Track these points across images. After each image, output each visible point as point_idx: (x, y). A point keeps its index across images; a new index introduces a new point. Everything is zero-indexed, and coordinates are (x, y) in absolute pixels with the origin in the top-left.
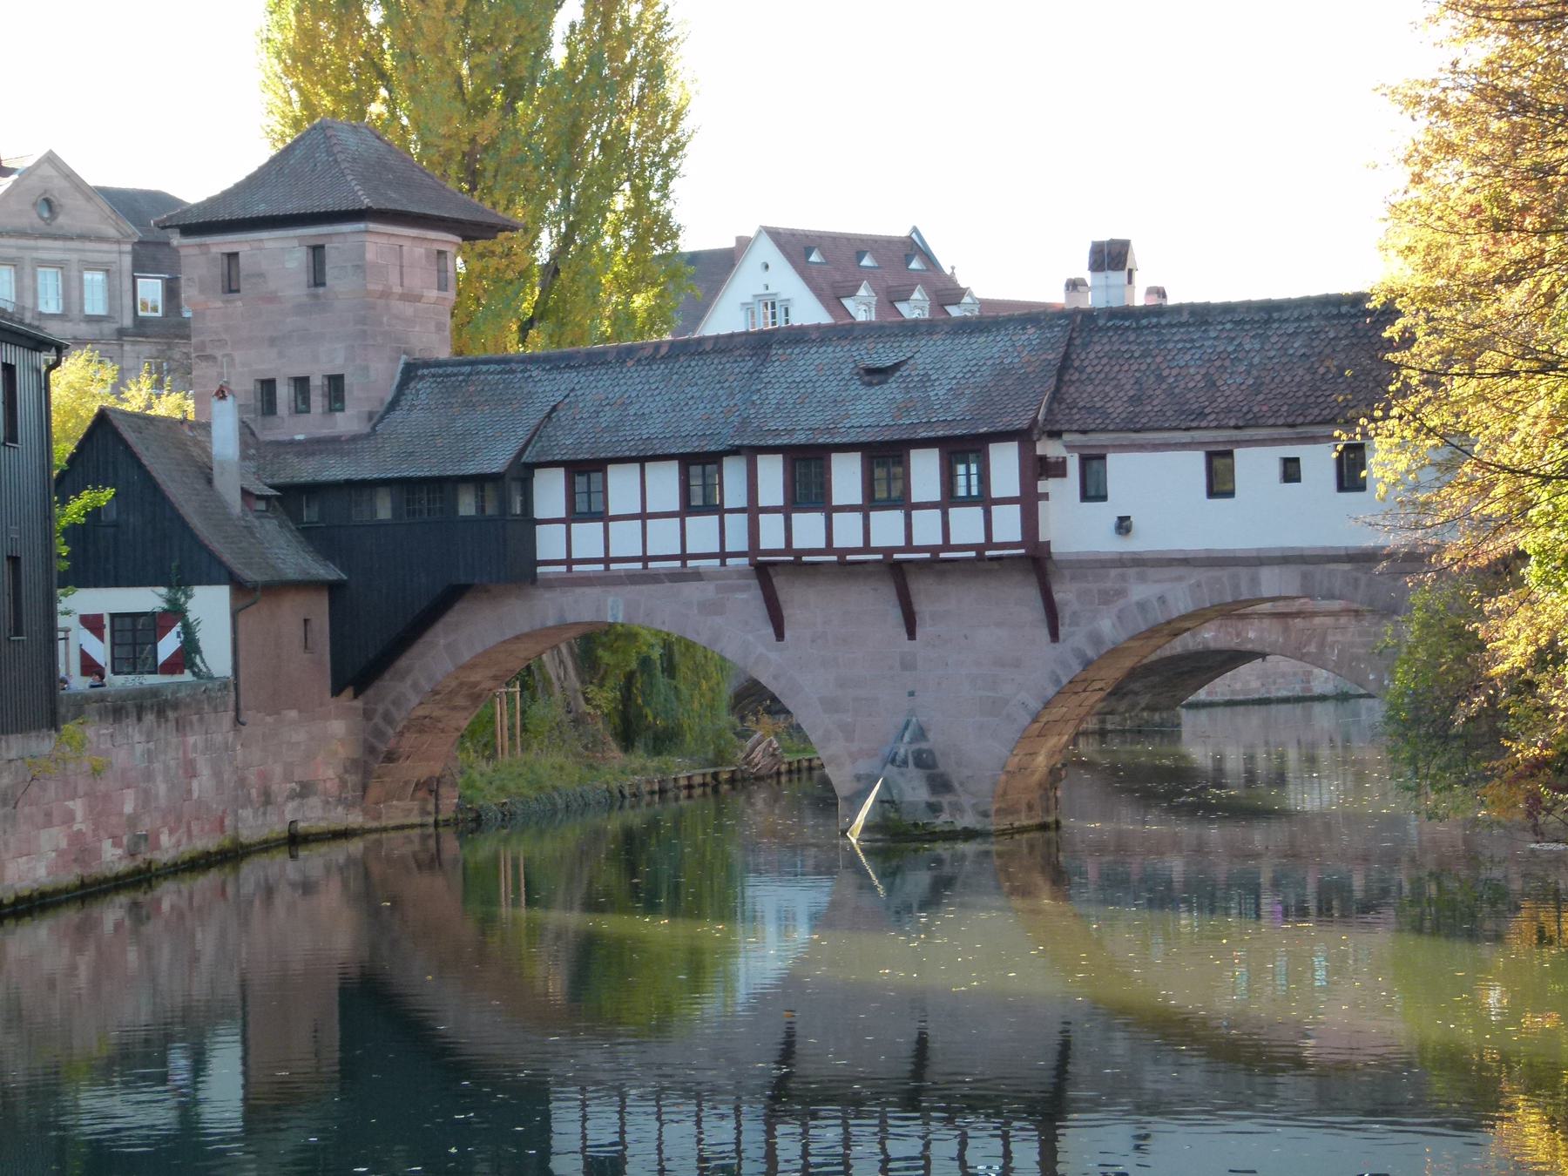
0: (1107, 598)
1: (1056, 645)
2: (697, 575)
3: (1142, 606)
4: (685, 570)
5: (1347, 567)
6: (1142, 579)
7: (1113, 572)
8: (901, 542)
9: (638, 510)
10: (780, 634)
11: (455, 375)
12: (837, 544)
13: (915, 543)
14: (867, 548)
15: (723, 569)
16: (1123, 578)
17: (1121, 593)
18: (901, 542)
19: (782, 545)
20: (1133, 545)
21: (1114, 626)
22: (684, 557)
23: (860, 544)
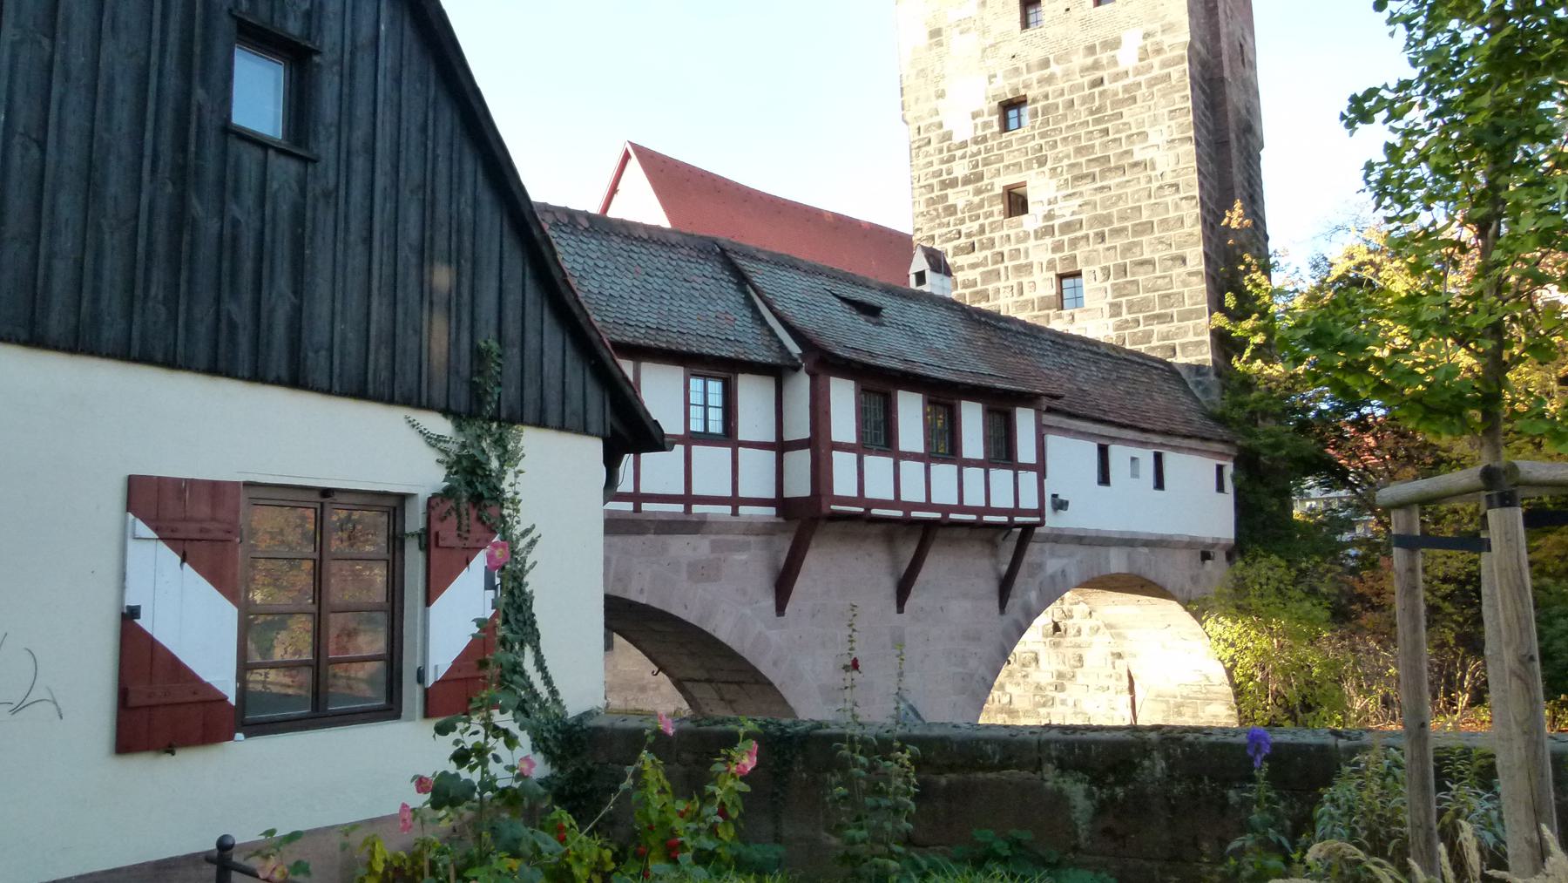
1: (1004, 617)
2: (696, 527)
4: (689, 518)
6: (1053, 555)
10: (780, 609)
12: (904, 498)
15: (734, 519)
17: (1041, 566)
18: (955, 502)
19: (854, 493)
22: (688, 499)
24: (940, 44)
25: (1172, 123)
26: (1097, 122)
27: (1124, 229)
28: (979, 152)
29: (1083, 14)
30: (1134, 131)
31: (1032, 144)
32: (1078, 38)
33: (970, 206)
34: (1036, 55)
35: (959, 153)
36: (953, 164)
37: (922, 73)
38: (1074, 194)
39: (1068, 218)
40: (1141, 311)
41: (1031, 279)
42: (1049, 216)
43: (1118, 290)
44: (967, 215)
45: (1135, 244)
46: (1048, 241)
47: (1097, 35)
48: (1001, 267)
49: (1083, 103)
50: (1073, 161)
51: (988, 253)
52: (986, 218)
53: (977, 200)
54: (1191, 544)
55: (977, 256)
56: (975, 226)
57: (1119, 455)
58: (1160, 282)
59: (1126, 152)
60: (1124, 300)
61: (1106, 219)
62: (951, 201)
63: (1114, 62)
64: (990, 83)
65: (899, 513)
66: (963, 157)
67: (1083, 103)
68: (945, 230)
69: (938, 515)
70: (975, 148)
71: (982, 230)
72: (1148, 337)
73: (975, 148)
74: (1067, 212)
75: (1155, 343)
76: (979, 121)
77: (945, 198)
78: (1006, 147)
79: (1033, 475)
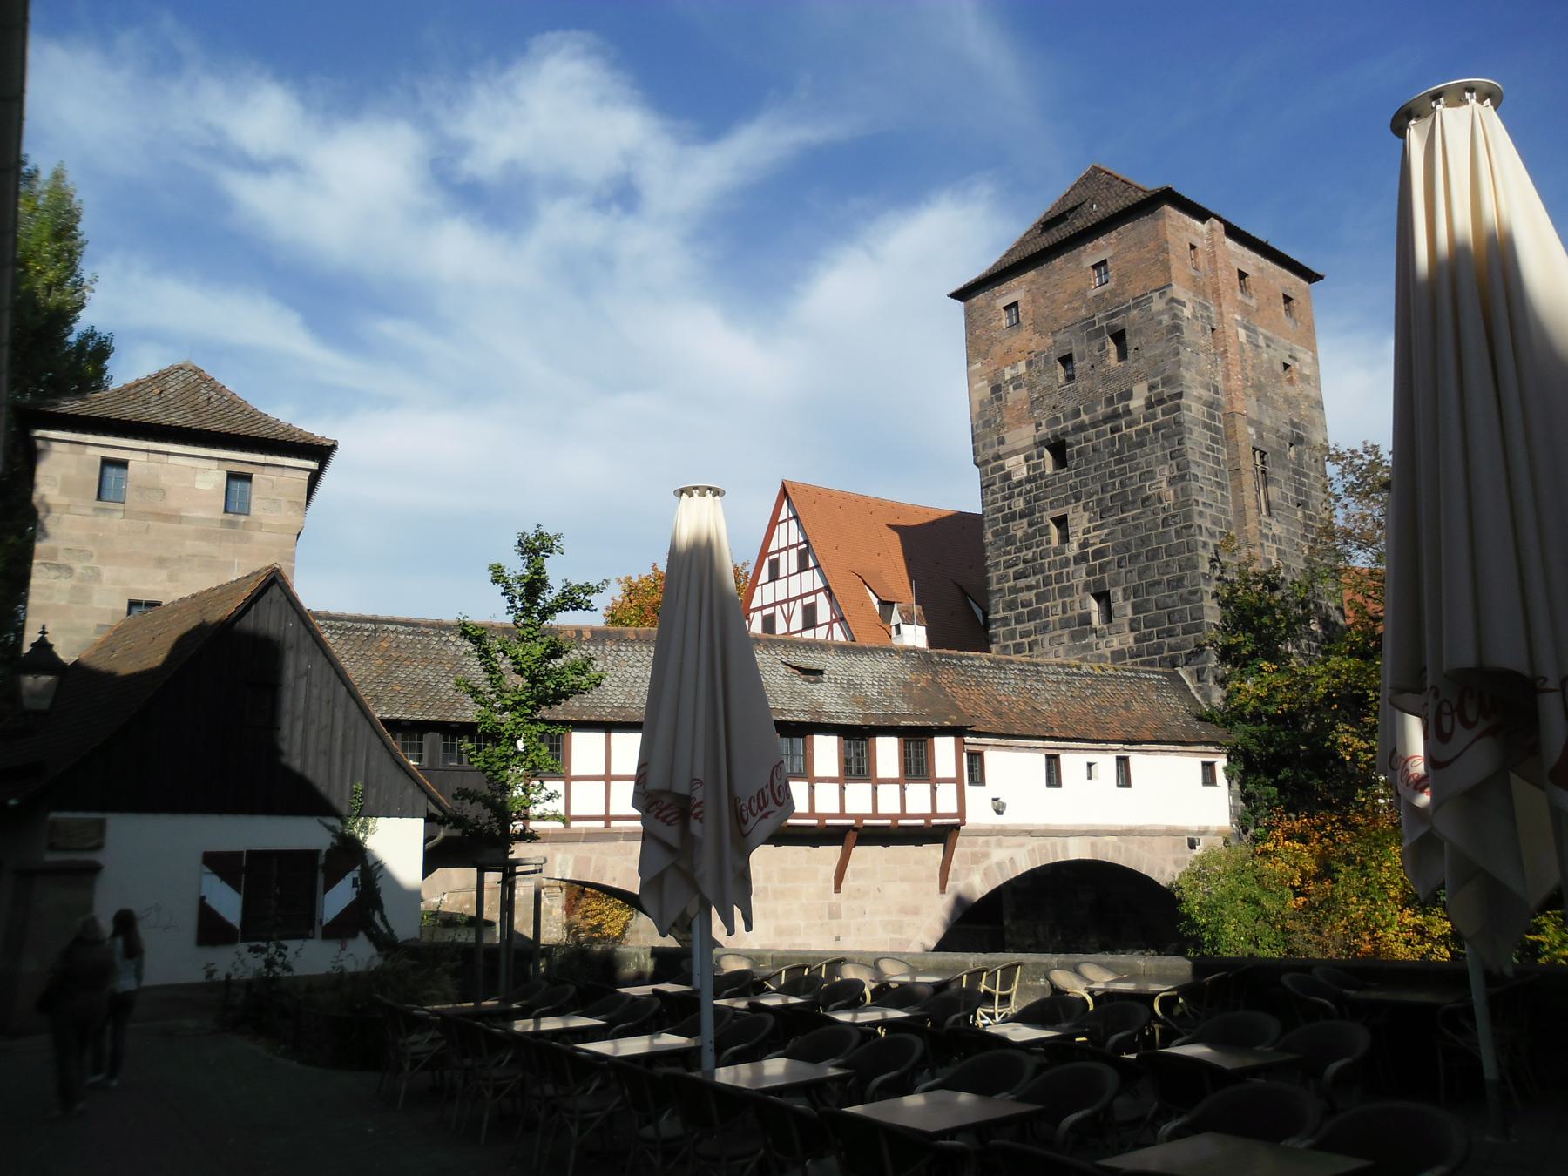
0: (977, 858)
1: (944, 895)
3: (1000, 865)
5: (1115, 838)
6: (999, 845)
7: (981, 839)
8: (869, 810)
9: (602, 772)
11: (357, 630)
12: (819, 809)
13: (881, 810)
14: (842, 814)
16: (987, 844)
17: (986, 855)
18: (869, 810)
20: (1007, 820)
21: (982, 881)
23: (836, 810)
24: (999, 398)
25: (1174, 463)
26: (1118, 462)
27: (1139, 555)
28: (1031, 491)
29: (1104, 370)
30: (1145, 469)
31: (1071, 481)
32: (1100, 391)
33: (1027, 537)
34: (1069, 406)
35: (1016, 491)
36: (1014, 500)
37: (987, 424)
38: (1102, 524)
39: (1098, 546)
40: (1153, 627)
41: (1071, 599)
42: (1084, 545)
43: (1137, 609)
44: (1024, 544)
45: (1148, 568)
46: (1084, 566)
47: (1115, 387)
48: (1050, 588)
49: (1106, 447)
50: (1100, 496)
51: (1039, 577)
52: (1038, 547)
53: (1030, 531)
54: (1171, 832)
55: (1032, 580)
56: (1030, 554)
57: (1072, 763)
58: (1168, 600)
59: (1140, 488)
60: (1142, 616)
61: (1127, 547)
62: (1012, 532)
63: (1128, 412)
64: (1037, 431)
65: (814, 822)
66: (1019, 494)
67: (1106, 447)
68: (1008, 557)
69: (852, 822)
70: (1028, 487)
71: (1034, 559)
72: (1160, 648)
73: (1028, 487)
74: (1098, 541)
75: (1165, 654)
76: (1031, 462)
77: (1006, 530)
78: (1051, 485)
79: (953, 787)
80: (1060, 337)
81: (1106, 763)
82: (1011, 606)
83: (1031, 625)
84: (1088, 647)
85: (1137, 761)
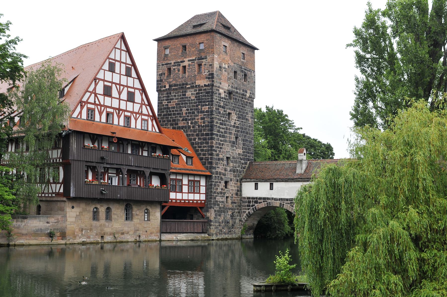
80: (235, 65)
81: (268, 184)
82: (219, 131)
83: (223, 139)
84: (234, 150)
85: (275, 185)
